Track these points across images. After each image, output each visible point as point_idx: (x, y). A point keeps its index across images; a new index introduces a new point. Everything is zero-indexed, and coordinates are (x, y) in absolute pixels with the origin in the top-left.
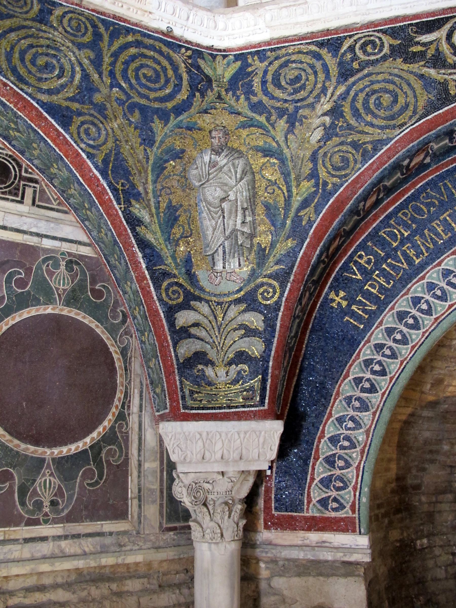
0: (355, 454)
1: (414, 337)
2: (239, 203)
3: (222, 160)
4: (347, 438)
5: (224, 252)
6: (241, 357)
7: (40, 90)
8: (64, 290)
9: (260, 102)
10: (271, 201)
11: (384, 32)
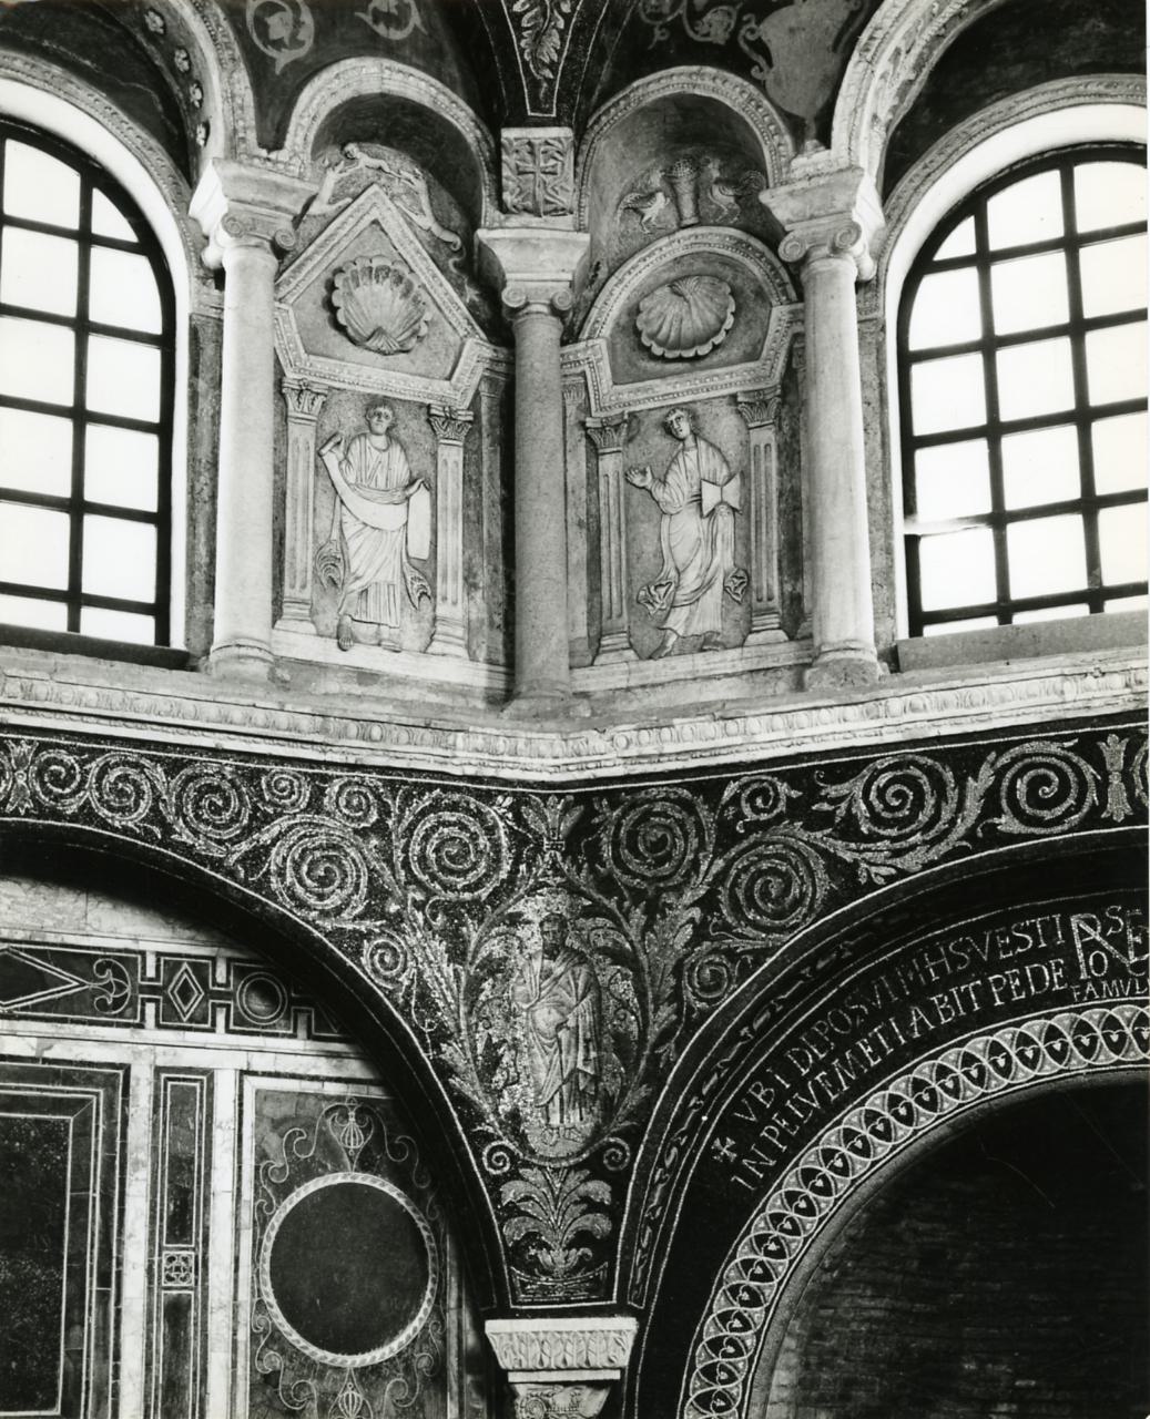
0: (741, 1362)
1: (823, 1205)
2: (581, 1033)
3: (558, 968)
4: (732, 1342)
5: (561, 1101)
6: (582, 1238)
7: (325, 914)
8: (355, 1150)
9: (610, 873)
10: (621, 1030)
11: (781, 776)
